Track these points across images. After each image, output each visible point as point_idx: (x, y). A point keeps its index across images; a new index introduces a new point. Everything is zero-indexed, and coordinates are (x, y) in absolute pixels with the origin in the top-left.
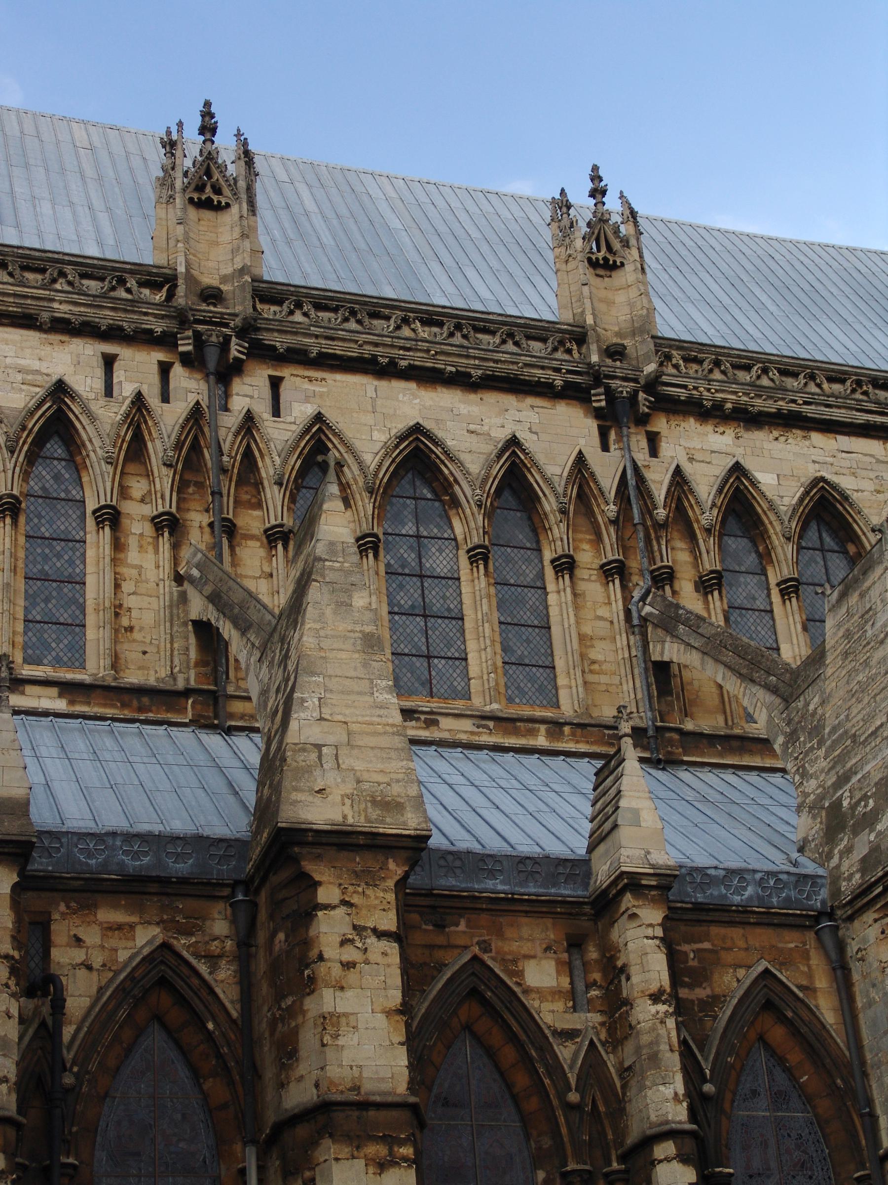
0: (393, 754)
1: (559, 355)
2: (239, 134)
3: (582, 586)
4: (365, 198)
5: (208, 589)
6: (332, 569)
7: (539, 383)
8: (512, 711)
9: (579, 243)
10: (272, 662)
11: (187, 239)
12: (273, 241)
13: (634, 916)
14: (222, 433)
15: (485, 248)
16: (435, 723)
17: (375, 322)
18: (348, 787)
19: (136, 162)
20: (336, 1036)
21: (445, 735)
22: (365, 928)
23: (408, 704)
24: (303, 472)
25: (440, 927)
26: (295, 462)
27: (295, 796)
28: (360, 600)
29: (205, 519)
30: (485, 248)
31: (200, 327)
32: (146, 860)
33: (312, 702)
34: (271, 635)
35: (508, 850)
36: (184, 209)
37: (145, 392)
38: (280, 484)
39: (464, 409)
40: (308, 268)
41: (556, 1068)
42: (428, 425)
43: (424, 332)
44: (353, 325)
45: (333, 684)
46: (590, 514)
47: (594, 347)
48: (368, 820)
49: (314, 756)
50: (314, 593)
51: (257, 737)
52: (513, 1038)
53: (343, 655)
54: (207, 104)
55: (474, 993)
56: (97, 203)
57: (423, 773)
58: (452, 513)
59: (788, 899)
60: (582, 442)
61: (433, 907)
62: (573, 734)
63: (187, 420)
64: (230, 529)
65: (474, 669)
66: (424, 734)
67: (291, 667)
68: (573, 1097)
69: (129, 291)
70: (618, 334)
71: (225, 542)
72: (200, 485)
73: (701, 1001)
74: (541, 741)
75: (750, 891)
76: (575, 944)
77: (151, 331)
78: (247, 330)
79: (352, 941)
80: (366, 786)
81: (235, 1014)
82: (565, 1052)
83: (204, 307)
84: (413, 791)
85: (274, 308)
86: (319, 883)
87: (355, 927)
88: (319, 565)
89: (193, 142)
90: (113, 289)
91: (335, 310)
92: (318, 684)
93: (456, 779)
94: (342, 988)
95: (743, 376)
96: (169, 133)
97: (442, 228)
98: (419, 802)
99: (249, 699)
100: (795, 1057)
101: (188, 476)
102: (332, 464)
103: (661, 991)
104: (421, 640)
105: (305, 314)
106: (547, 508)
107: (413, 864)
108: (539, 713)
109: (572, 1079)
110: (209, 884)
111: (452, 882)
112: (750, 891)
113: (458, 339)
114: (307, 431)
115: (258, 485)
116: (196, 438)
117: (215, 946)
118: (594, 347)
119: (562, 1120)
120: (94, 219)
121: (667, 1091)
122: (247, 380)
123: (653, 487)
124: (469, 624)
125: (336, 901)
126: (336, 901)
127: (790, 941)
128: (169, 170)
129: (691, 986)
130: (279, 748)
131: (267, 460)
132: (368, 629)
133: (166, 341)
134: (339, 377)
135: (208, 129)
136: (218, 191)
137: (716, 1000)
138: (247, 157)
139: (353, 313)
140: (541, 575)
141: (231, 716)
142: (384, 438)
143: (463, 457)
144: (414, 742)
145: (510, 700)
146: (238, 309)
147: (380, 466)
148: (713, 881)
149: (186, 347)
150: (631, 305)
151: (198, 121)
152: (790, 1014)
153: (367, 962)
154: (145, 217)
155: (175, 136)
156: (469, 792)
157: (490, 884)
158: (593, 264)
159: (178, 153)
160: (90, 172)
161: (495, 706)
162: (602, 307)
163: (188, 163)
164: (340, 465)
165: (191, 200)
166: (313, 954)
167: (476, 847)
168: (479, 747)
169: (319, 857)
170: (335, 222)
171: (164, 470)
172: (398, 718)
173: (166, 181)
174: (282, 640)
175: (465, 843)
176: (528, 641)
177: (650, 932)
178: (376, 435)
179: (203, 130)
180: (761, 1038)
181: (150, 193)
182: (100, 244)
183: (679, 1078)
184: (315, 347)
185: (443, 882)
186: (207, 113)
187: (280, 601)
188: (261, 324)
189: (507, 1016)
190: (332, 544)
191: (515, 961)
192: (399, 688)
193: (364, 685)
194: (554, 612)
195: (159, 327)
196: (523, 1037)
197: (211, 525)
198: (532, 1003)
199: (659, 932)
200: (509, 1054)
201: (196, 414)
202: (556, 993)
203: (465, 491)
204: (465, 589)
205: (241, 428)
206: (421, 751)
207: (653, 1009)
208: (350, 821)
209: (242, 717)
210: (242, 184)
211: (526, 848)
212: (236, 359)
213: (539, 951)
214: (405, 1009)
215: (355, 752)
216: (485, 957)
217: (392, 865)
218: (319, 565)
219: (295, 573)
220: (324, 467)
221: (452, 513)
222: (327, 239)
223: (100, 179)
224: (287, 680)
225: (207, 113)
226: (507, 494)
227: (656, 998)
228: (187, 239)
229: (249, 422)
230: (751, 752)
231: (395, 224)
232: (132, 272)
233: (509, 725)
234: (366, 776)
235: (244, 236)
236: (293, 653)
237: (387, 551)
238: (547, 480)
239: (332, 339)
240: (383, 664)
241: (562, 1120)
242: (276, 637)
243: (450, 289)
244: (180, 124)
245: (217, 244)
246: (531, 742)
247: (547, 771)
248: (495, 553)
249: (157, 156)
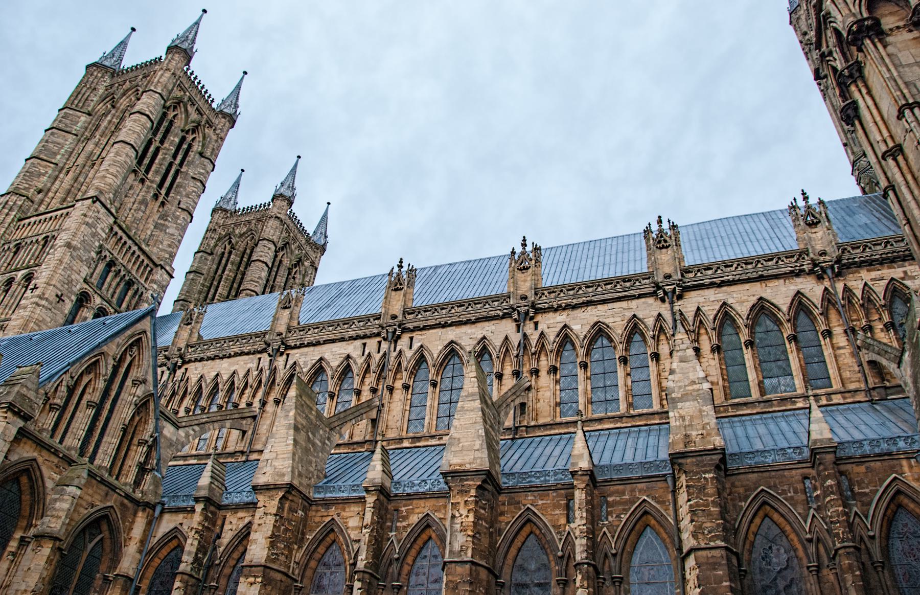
7: (495, 316)
32: (250, 498)
39: (469, 331)
61: (326, 504)
75: (428, 487)
95: (571, 293)
129: (401, 522)
230: (554, 429)
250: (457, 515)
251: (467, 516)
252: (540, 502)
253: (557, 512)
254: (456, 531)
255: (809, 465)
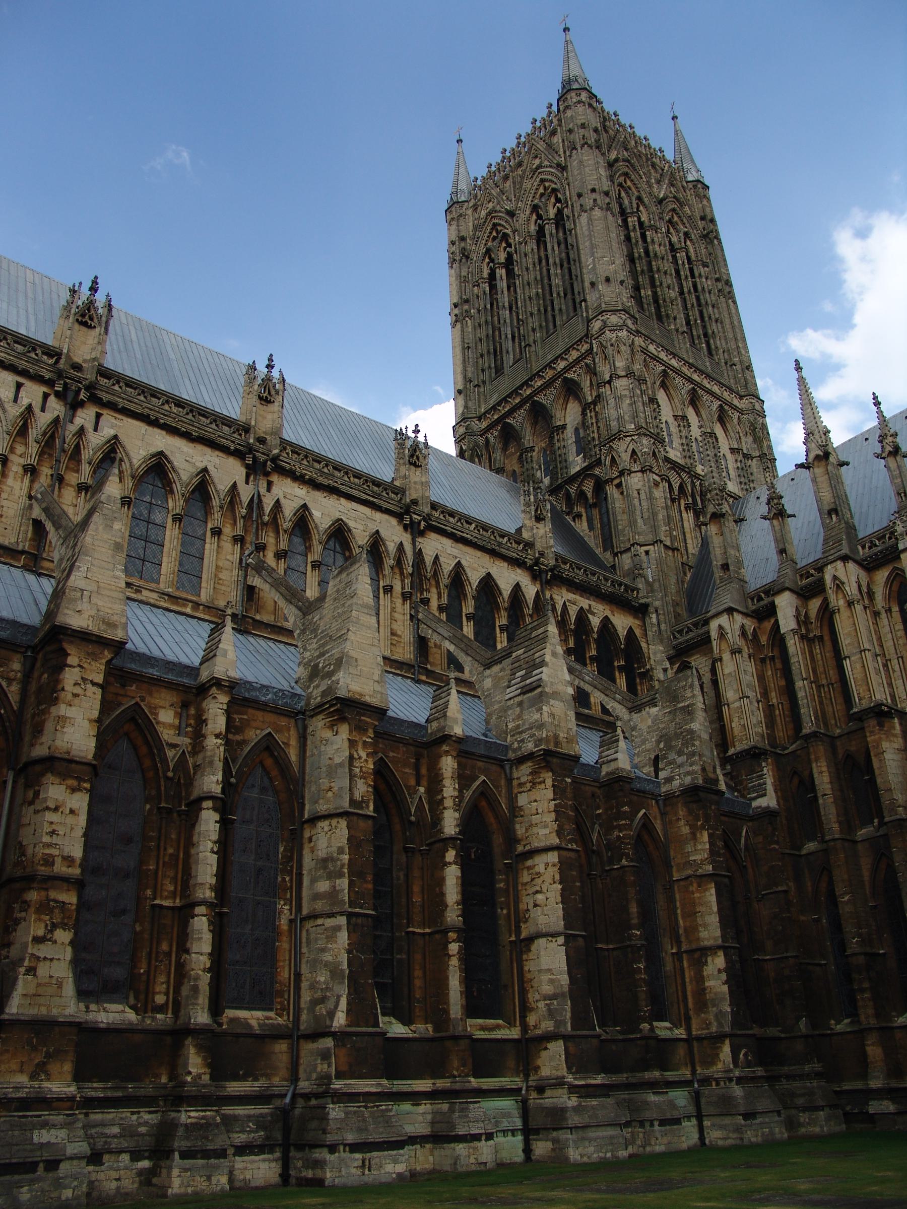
0: (118, 601)
1: (235, 435)
2: (108, 296)
3: (222, 543)
4: (161, 342)
5: (44, 505)
6: (107, 508)
8: (178, 594)
9: (256, 387)
10: (68, 547)
11: (71, 338)
12: (113, 349)
13: (215, 698)
14: (67, 433)
15: (212, 379)
16: (141, 592)
17: (153, 399)
18: (93, 613)
19: (55, 296)
20: (63, 727)
21: (144, 598)
22: (87, 680)
23: (129, 580)
24: (102, 461)
25: (123, 686)
26: (100, 455)
27: (66, 611)
28: (117, 526)
29: (50, 472)
30: (212, 379)
31: (68, 381)
33: (84, 568)
34: (70, 533)
35: (163, 657)
36: (73, 323)
37: (33, 405)
38: (90, 464)
40: (126, 366)
41: (164, 760)
42: (167, 453)
43: (175, 410)
44: (142, 398)
45: (95, 562)
46: (233, 511)
47: (252, 436)
48: (99, 629)
49: (79, 594)
50: (96, 518)
51: (53, 581)
52: (147, 743)
53: (104, 550)
54: (96, 278)
55: (133, 720)
56: (31, 310)
57: (130, 614)
58: (169, 496)
59: (286, 703)
60: (237, 477)
62: (204, 610)
63: (51, 423)
64: (61, 480)
65: (163, 571)
66: (134, 596)
67: (77, 550)
68: (170, 774)
69: (36, 355)
70: (265, 433)
71: (57, 484)
72: (51, 455)
73: (237, 741)
74: (188, 610)
75: (270, 696)
76: (185, 705)
77: (43, 377)
78: (90, 387)
79: (80, 684)
80: (101, 613)
81: (15, 708)
82: (170, 753)
83: (72, 371)
84: (123, 620)
85: (106, 380)
86: (69, 655)
87: (82, 678)
88: (101, 505)
89: (85, 293)
90: (29, 352)
91: (135, 389)
92: (88, 561)
93: (144, 619)
94: (70, 705)
96: (74, 286)
97: (194, 365)
98: (125, 626)
99: (53, 562)
100: (274, 773)
101: (46, 450)
102: (118, 459)
103: (220, 734)
104: (141, 552)
105: (120, 387)
106: (214, 504)
107: (117, 654)
108: (190, 597)
109: (171, 765)
110: (15, 644)
111: (133, 666)
112: (270, 696)
113: (190, 417)
114: (109, 442)
115: (79, 462)
116: (53, 433)
117: (12, 675)
118: (252, 436)
119: (163, 783)
120: (27, 317)
121: (214, 779)
122: (85, 411)
123: (265, 505)
124: (166, 549)
125: (76, 664)
126: (76, 664)
127: (283, 722)
128: (70, 303)
129: (234, 734)
130: (63, 587)
131: (86, 451)
132: (118, 540)
133: (50, 383)
134: (130, 420)
135: (94, 289)
136: (91, 319)
137: (244, 742)
138: (110, 307)
139: (143, 392)
140: (204, 534)
141: (42, 568)
142: (145, 454)
143: (180, 471)
144: (129, 598)
145: (178, 588)
146: (88, 376)
147: (140, 466)
148: (255, 689)
149: (58, 388)
150: (273, 421)
151: (90, 284)
152: (276, 754)
153: (85, 695)
154: (53, 322)
155: (76, 288)
156: (150, 627)
157: (151, 671)
158: (260, 398)
159: (76, 297)
160: (30, 295)
161: (170, 590)
162: (260, 418)
163: (80, 303)
164: (121, 460)
165: (77, 320)
166: (60, 687)
167: (148, 653)
168: (158, 607)
169: (71, 642)
170: (144, 348)
171: (35, 444)
172: (124, 585)
173: (67, 308)
174: (75, 536)
175: (142, 649)
176: (192, 563)
177: (221, 706)
178: (141, 452)
179: (91, 289)
180: (261, 762)
181: (58, 312)
182: (27, 329)
183: (220, 774)
184: (121, 403)
185: (129, 665)
186: (95, 282)
187: (78, 519)
188: (98, 386)
189: (146, 732)
190: (109, 496)
191: (155, 708)
192: (126, 571)
193: (111, 566)
194: (207, 552)
195: (47, 376)
196: (152, 744)
197: (52, 475)
198: (160, 729)
199: (225, 707)
200: (144, 750)
201: (56, 421)
202: (171, 726)
203: (178, 488)
204: (168, 533)
205: (77, 433)
206: (131, 603)
207: (215, 741)
208: (90, 628)
209: (47, 569)
210: (104, 319)
211: (171, 657)
212: (82, 400)
213: (167, 705)
214: (99, 721)
215: (100, 596)
216: (142, 704)
217: (106, 652)
218: (101, 505)
219: (88, 506)
220: (113, 460)
221: (169, 496)
222: (139, 356)
223: (35, 299)
224: (73, 556)
225: (95, 282)
226: (197, 493)
227: (217, 736)
228: (71, 338)
229: (81, 431)
231: (172, 356)
232: (40, 346)
233: (175, 600)
234: (102, 609)
235: (99, 343)
236: (79, 544)
237: (134, 507)
238: (217, 491)
239: (131, 402)
240: (121, 557)
241: (163, 783)
242: (72, 535)
243: (191, 392)
244: (81, 283)
245: (85, 343)
246: (183, 610)
247: (188, 625)
248: (185, 520)
249: (66, 295)
250: (356, 756)
251: (366, 761)
252: (391, 754)
253: (407, 770)
254: (355, 776)
255: (597, 784)
